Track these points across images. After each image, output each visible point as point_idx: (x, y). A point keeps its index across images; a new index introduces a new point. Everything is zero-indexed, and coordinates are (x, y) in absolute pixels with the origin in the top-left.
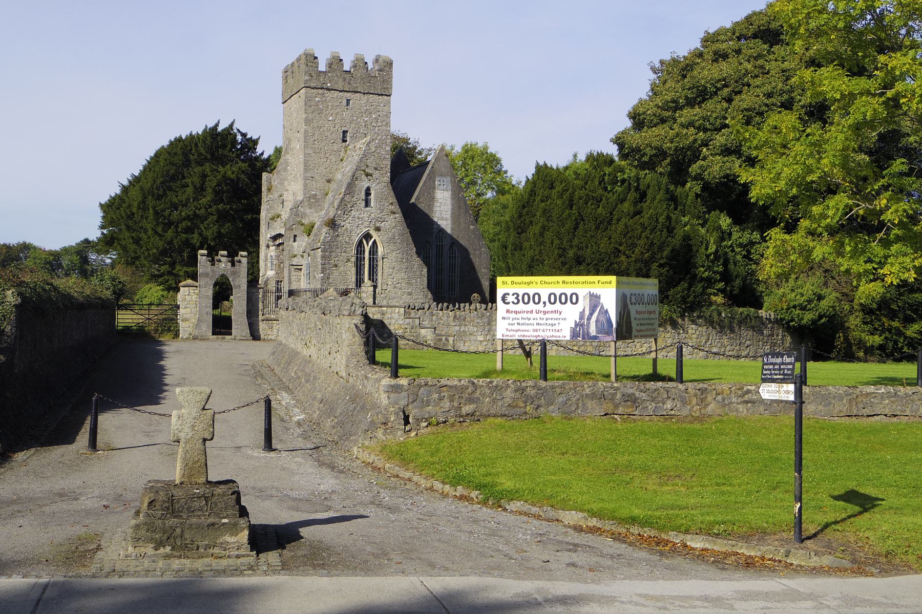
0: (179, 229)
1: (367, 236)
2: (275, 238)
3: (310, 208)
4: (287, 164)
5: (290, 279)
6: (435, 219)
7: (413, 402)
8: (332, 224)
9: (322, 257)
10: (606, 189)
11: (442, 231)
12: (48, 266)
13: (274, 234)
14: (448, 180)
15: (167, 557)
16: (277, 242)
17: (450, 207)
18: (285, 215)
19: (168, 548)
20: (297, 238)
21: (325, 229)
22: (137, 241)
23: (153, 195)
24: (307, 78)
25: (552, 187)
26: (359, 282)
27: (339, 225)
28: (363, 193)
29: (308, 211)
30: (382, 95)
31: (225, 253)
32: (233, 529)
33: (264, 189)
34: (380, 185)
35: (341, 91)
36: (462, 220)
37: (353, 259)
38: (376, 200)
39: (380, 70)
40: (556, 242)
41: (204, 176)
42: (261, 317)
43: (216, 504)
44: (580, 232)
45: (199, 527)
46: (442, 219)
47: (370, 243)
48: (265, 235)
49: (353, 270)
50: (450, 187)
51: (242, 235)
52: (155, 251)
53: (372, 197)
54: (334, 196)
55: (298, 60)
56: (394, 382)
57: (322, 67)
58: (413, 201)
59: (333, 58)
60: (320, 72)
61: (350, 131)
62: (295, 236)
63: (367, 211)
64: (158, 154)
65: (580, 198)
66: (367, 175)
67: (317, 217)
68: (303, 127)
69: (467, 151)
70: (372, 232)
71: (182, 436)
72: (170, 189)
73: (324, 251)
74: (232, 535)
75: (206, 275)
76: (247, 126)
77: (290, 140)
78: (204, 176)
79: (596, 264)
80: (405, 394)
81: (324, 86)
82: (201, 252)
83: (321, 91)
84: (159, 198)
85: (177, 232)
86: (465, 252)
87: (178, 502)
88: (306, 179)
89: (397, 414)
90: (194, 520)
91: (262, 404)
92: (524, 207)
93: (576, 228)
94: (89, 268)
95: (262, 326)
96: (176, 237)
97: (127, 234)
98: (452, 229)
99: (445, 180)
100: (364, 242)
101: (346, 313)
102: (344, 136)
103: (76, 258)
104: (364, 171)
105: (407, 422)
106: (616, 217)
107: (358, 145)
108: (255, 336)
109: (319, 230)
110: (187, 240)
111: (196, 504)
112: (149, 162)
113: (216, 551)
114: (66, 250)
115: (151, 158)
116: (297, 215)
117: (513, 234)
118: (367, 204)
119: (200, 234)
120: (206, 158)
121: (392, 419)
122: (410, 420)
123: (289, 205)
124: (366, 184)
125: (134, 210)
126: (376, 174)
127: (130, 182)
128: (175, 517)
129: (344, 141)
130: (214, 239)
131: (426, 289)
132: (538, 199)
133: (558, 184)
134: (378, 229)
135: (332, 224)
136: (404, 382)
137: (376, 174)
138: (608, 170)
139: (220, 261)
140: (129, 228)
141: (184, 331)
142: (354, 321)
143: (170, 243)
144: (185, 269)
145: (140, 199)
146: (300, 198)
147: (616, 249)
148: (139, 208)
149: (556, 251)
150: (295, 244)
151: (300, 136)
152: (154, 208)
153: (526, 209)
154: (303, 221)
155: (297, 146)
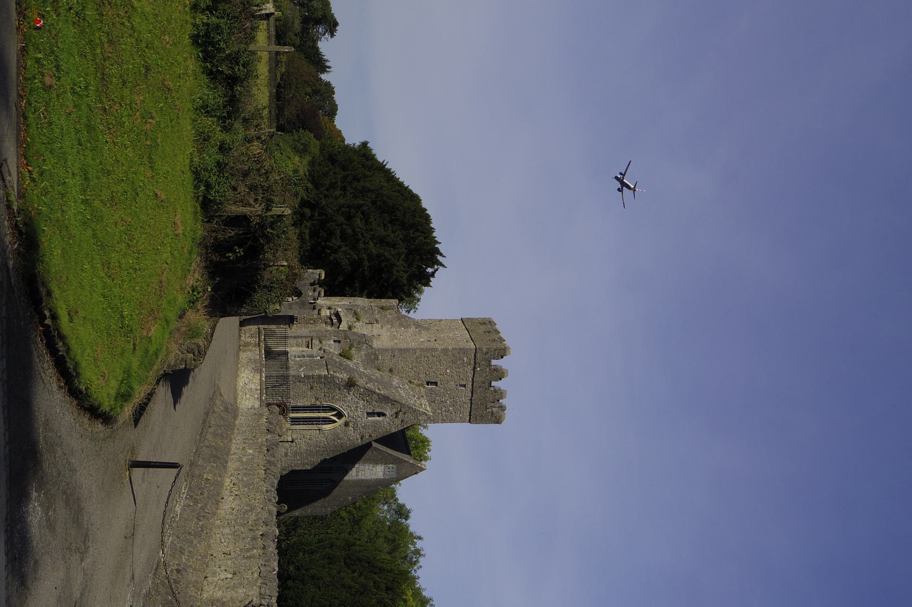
1: (340, 415)
2: (337, 315)
3: (366, 355)
5: (298, 337)
6: (357, 466)
8: (350, 384)
9: (320, 376)
11: (346, 472)
16: (333, 318)
17: (369, 478)
18: (361, 328)
20: (337, 344)
21: (345, 376)
22: (333, 186)
27: (349, 390)
33: (384, 302)
34: (388, 424)
37: (318, 403)
38: (374, 422)
39: (492, 413)
40: (337, 602)
41: (394, 246)
46: (357, 472)
48: (340, 303)
49: (308, 404)
50: (387, 477)
55: (502, 340)
58: (375, 444)
59: (503, 373)
60: (490, 362)
62: (339, 342)
64: (415, 199)
66: (397, 414)
69: (423, 442)
70: (343, 420)
76: (441, 279)
77: (428, 329)
78: (394, 246)
83: (472, 362)
85: (341, 224)
86: (326, 493)
88: (393, 350)
92: (369, 563)
95: (253, 328)
96: (337, 225)
98: (348, 481)
100: (334, 413)
103: (319, 14)
107: (424, 401)
115: (410, 191)
116: (359, 343)
118: (369, 414)
124: (388, 412)
126: (398, 421)
129: (428, 383)
131: (290, 469)
132: (376, 577)
134: (346, 424)
135: (350, 384)
137: (398, 421)
139: (314, 291)
142: (255, 599)
144: (307, 231)
146: (376, 344)
148: (364, 187)
150: (332, 342)
151: (431, 345)
152: (362, 205)
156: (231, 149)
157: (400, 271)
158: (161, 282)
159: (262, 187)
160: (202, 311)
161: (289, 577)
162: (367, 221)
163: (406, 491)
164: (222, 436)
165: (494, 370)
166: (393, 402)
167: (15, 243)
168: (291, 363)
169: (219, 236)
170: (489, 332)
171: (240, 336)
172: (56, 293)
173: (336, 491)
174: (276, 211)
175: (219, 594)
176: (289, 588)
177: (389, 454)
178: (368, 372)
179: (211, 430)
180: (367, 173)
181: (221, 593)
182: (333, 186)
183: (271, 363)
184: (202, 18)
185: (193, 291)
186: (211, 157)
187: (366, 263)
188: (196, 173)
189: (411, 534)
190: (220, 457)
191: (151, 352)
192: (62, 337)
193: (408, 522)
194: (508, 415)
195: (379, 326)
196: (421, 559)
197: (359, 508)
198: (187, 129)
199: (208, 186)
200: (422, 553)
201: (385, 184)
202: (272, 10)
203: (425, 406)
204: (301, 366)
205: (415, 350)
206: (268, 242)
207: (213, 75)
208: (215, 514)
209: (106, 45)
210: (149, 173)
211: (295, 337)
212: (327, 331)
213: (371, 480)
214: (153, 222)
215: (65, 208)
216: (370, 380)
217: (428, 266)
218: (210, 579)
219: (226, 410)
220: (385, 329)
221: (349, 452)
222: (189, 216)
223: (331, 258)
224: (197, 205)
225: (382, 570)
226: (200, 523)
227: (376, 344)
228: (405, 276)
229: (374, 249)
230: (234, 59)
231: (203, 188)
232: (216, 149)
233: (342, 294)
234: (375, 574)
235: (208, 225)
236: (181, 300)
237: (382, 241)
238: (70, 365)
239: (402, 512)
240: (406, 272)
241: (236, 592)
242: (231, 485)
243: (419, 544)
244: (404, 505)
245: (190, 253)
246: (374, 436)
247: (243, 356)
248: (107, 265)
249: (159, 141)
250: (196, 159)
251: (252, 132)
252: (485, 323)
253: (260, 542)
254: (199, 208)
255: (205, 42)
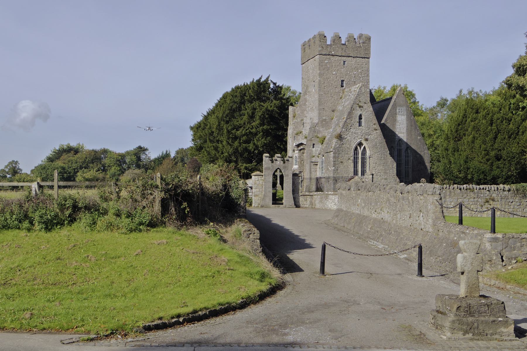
0: (241, 141)
2: (298, 146)
3: (323, 127)
4: (306, 100)
5: (310, 171)
6: (397, 133)
7: (505, 248)
8: (340, 137)
9: (334, 157)
10: (512, 112)
11: (400, 140)
12: (118, 162)
13: (298, 143)
14: (404, 108)
15: (472, 339)
16: (300, 148)
18: (306, 131)
19: (470, 335)
20: (315, 146)
21: (335, 140)
22: (216, 149)
23: (224, 121)
24: (320, 49)
25: (477, 112)
26: (356, 173)
28: (358, 118)
29: (321, 129)
30: (365, 58)
31: (279, 155)
32: (506, 323)
33: (290, 116)
34: (368, 112)
35: (340, 56)
36: (413, 133)
37: (352, 158)
38: (365, 122)
39: (363, 43)
40: (483, 146)
41: (255, 109)
42: (300, 194)
43: (493, 309)
44: (498, 140)
45: (486, 322)
46: (401, 133)
47: (362, 148)
48: (291, 144)
49: (352, 165)
50: (405, 113)
51: (277, 144)
52: (226, 154)
53: (363, 120)
54: (338, 120)
55: (314, 37)
56: (493, 236)
58: (383, 122)
59: (336, 36)
60: (328, 45)
61: (346, 80)
62: (314, 144)
63: (360, 129)
65: (498, 119)
67: (328, 133)
68: (317, 79)
71: (466, 269)
72: (234, 117)
73: (334, 153)
74: (505, 327)
75: (268, 169)
77: (307, 87)
79: (509, 161)
80: (500, 243)
81: (330, 54)
82: (265, 155)
83: (328, 57)
84: (227, 122)
85: (240, 143)
87: (473, 308)
88: (320, 110)
89: (497, 255)
90: (482, 318)
91: (417, 249)
92: (459, 125)
93: (495, 138)
94: (141, 163)
95: (301, 199)
96: (240, 146)
97: (210, 145)
98: (407, 139)
99: (403, 109)
101: (430, 193)
102: (342, 84)
103: (134, 158)
104: (358, 104)
105: (503, 261)
106: (521, 131)
108: (297, 205)
109: (330, 140)
110: (246, 148)
111: (483, 309)
112: (219, 102)
113: (497, 336)
114: (128, 153)
115: (221, 99)
116: (315, 132)
117: (452, 142)
118: (360, 125)
119: (254, 144)
120: (254, 98)
121: (494, 258)
122: (504, 259)
123: (307, 127)
124: (358, 112)
125: (214, 130)
127: (208, 114)
128: (472, 316)
129: (342, 86)
130: (263, 147)
131: (396, 176)
132: (469, 120)
133: (482, 110)
134: (366, 140)
135: (340, 137)
136: (500, 236)
137: (365, 106)
138: (512, 101)
139: (276, 160)
140: (211, 141)
141: (256, 202)
142: (435, 198)
143: (237, 149)
144: (245, 165)
145: (217, 123)
146: (316, 121)
147: (523, 150)
148: (217, 129)
149: (483, 152)
150: (314, 149)
151: (317, 84)
152: (227, 129)
153: (460, 126)
154: (318, 135)
155: (313, 90)
156: (118, 210)
157: (271, 105)
158: (193, 253)
159: (143, 190)
160: (229, 229)
161: (466, 177)
162: (237, 128)
163: (426, 101)
164: (350, 218)
165: (334, 42)
166: (352, 109)
167: (118, 337)
168: (326, 175)
169: (174, 217)
170: (309, 46)
171: (306, 207)
172: (161, 314)
173: (414, 147)
174: (158, 182)
175: (430, 221)
176: (473, 178)
177: (390, 112)
178: (333, 126)
179: (346, 226)
180: (208, 127)
181: (430, 220)
182: (216, 149)
183: (325, 189)
184: (37, 227)
185: (208, 234)
186: (125, 221)
187: (265, 127)
188: (131, 231)
189: (458, 97)
190: (361, 220)
191: (239, 260)
192: (195, 312)
193: (449, 99)
194: (366, 32)
195: (305, 118)
196: (475, 90)
197: (435, 132)
198: (106, 235)
199: (141, 224)
200: (471, 90)
201: (216, 115)
202: (36, 183)
203: (355, 88)
204: (328, 169)
205: (320, 95)
206: (181, 186)
207: (72, 220)
208: (390, 224)
209: (35, 283)
210: (122, 259)
211: (311, 173)
212: (307, 153)
214: (153, 258)
215: (112, 308)
216: (338, 124)
217: (269, 87)
218: (423, 227)
219: (337, 216)
220: (307, 115)
221: (385, 138)
222: (158, 235)
223: (261, 150)
224: (152, 230)
225: (465, 116)
226: (393, 233)
227: (316, 121)
228: (274, 102)
229: (257, 122)
230: (62, 207)
231: (141, 227)
232: (118, 219)
233: (285, 143)
234: (466, 121)
235: (167, 223)
236: (213, 240)
237: (252, 117)
238: (218, 308)
239: (442, 104)
240: (272, 101)
241: (430, 210)
242: (376, 213)
243: (465, 92)
244: (438, 102)
245: (182, 235)
246: (376, 122)
247: (318, 206)
248: (167, 285)
249: (103, 252)
250: (124, 230)
251: (114, 196)
252: (304, 49)
253: (405, 195)
254: (155, 229)
255: (50, 225)
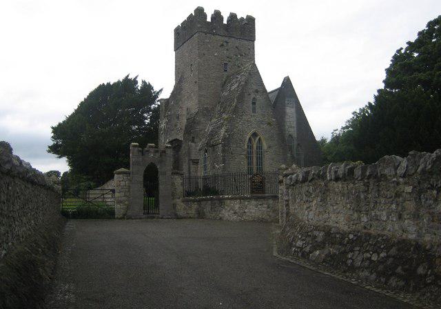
2: (171, 142)
9: (223, 151)
17: (295, 119)
49: (246, 162)
57: (209, 19)
73: (224, 146)
146: (194, 110)
204: (214, 167)
213: (297, 118)
